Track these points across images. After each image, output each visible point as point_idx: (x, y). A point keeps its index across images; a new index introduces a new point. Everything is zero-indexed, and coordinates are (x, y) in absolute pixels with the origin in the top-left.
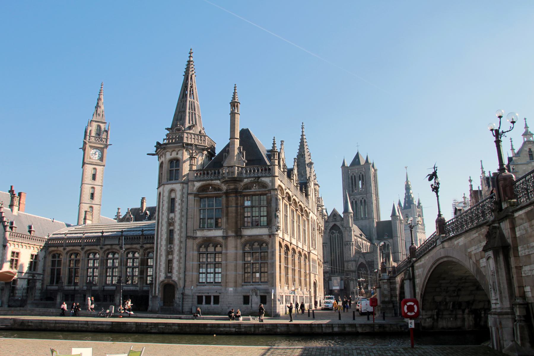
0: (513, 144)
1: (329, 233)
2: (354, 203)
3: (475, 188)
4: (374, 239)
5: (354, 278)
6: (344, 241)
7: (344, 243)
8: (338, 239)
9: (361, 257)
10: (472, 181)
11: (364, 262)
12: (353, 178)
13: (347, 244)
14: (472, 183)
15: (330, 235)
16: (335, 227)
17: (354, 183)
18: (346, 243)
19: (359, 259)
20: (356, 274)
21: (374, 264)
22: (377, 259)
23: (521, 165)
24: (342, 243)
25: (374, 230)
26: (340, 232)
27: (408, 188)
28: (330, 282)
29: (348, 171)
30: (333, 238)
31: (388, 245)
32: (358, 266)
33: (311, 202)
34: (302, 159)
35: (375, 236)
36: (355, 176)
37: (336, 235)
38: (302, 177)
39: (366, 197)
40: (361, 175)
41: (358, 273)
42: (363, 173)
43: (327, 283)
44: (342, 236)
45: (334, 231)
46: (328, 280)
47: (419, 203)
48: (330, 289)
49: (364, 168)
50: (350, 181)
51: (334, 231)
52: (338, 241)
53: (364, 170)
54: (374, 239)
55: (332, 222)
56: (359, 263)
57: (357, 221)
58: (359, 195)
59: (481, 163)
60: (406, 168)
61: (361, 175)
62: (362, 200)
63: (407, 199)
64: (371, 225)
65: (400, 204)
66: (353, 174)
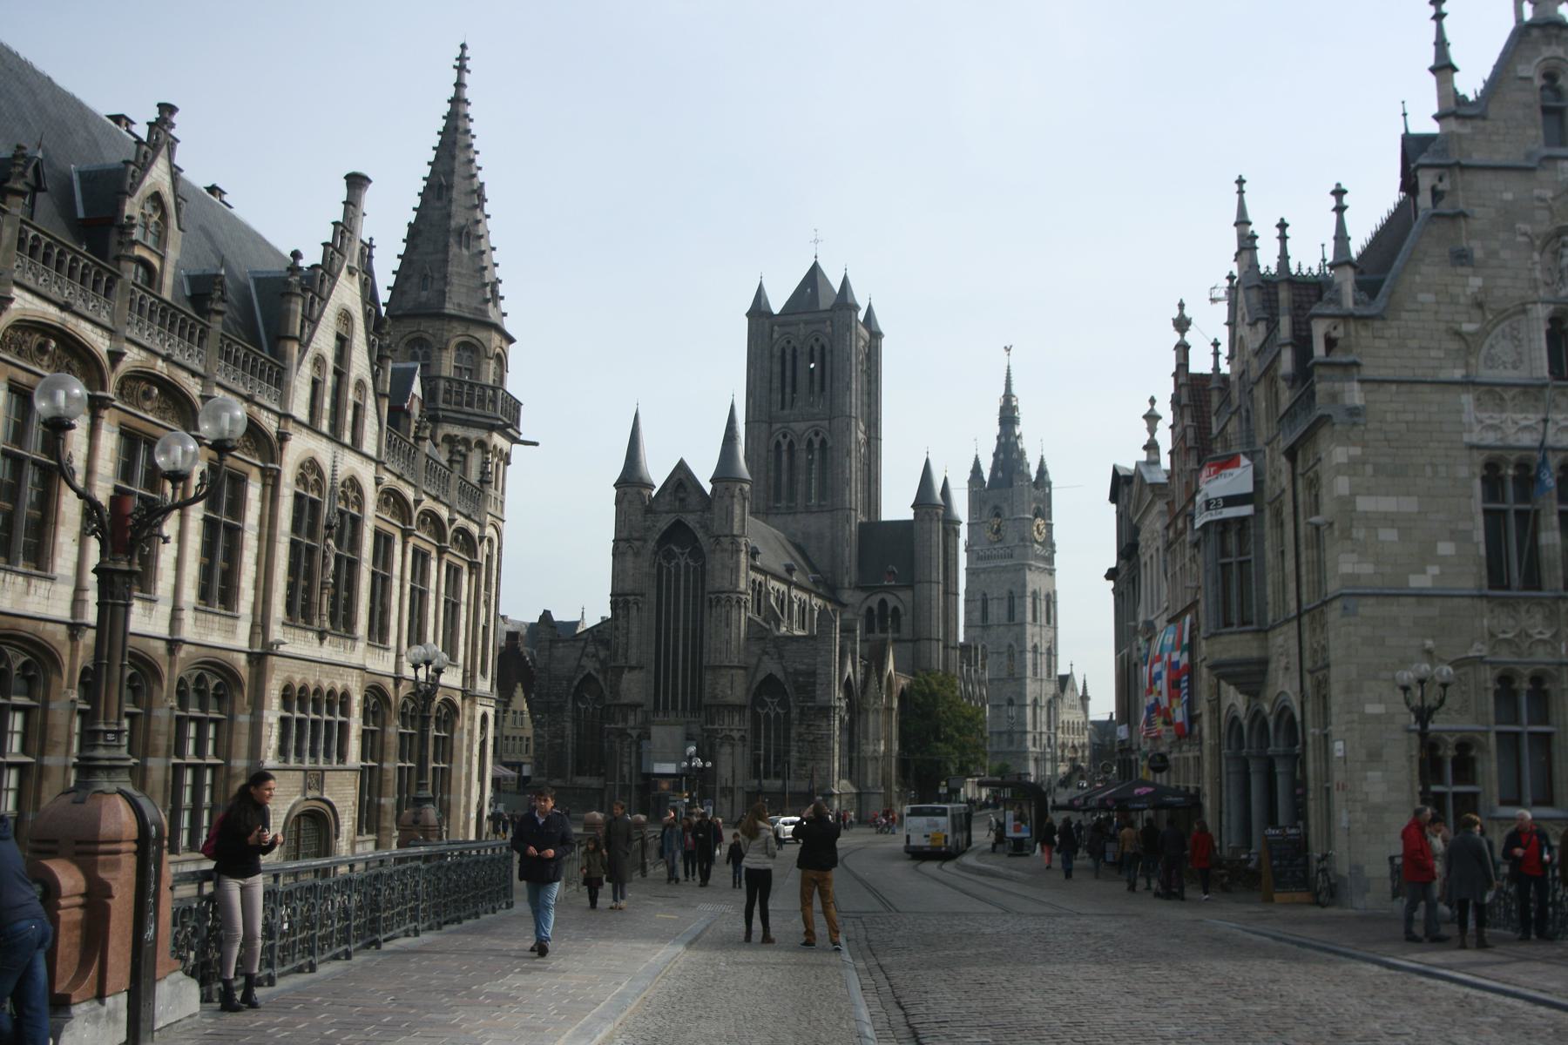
0: (1449, 35)
1: (656, 553)
2: (784, 447)
3: (1200, 363)
4: (846, 585)
5: (736, 735)
6: (708, 588)
7: (706, 598)
8: (687, 581)
9: (767, 653)
10: (1188, 323)
11: (780, 675)
12: (788, 357)
13: (718, 601)
14: (1188, 337)
15: (660, 564)
16: (678, 533)
17: (788, 374)
18: (713, 596)
19: (760, 660)
20: (748, 713)
21: (814, 684)
22: (828, 664)
23: (1489, 175)
24: (703, 596)
25: (847, 553)
26: (698, 553)
27: (1008, 417)
28: (644, 743)
29: (772, 331)
30: (669, 569)
31: (896, 609)
32: (754, 686)
33: (316, 384)
34: (438, 204)
35: (850, 576)
36: (794, 350)
37: (682, 564)
38: (424, 288)
39: (830, 431)
40: (817, 348)
41: (756, 719)
42: (824, 340)
43: (634, 749)
44: (703, 565)
45: (675, 548)
46: (639, 736)
47: (1042, 471)
48: (644, 770)
49: (828, 323)
50: (777, 368)
51: (675, 548)
52: (687, 588)
53: (829, 330)
54: (846, 585)
55: (667, 513)
56: (760, 676)
57: (790, 518)
58: (804, 420)
59: (1241, 192)
60: (1008, 349)
61: (817, 348)
62: (814, 438)
63: (1001, 456)
64: (840, 534)
65: (977, 470)
66: (789, 342)
